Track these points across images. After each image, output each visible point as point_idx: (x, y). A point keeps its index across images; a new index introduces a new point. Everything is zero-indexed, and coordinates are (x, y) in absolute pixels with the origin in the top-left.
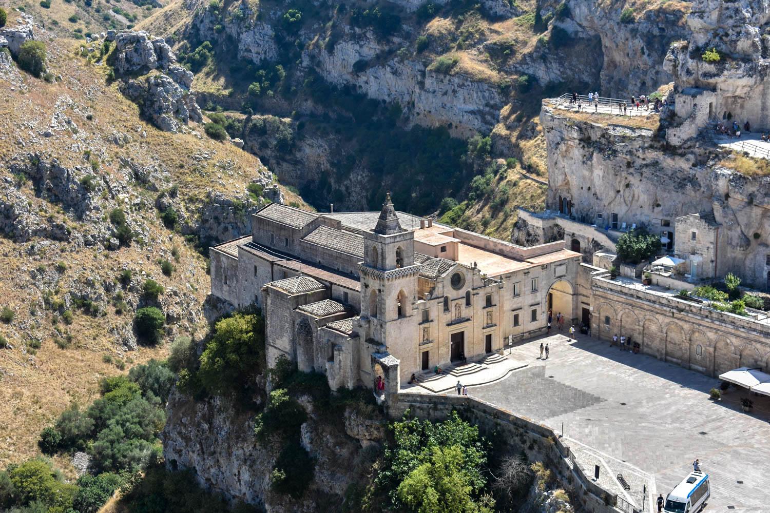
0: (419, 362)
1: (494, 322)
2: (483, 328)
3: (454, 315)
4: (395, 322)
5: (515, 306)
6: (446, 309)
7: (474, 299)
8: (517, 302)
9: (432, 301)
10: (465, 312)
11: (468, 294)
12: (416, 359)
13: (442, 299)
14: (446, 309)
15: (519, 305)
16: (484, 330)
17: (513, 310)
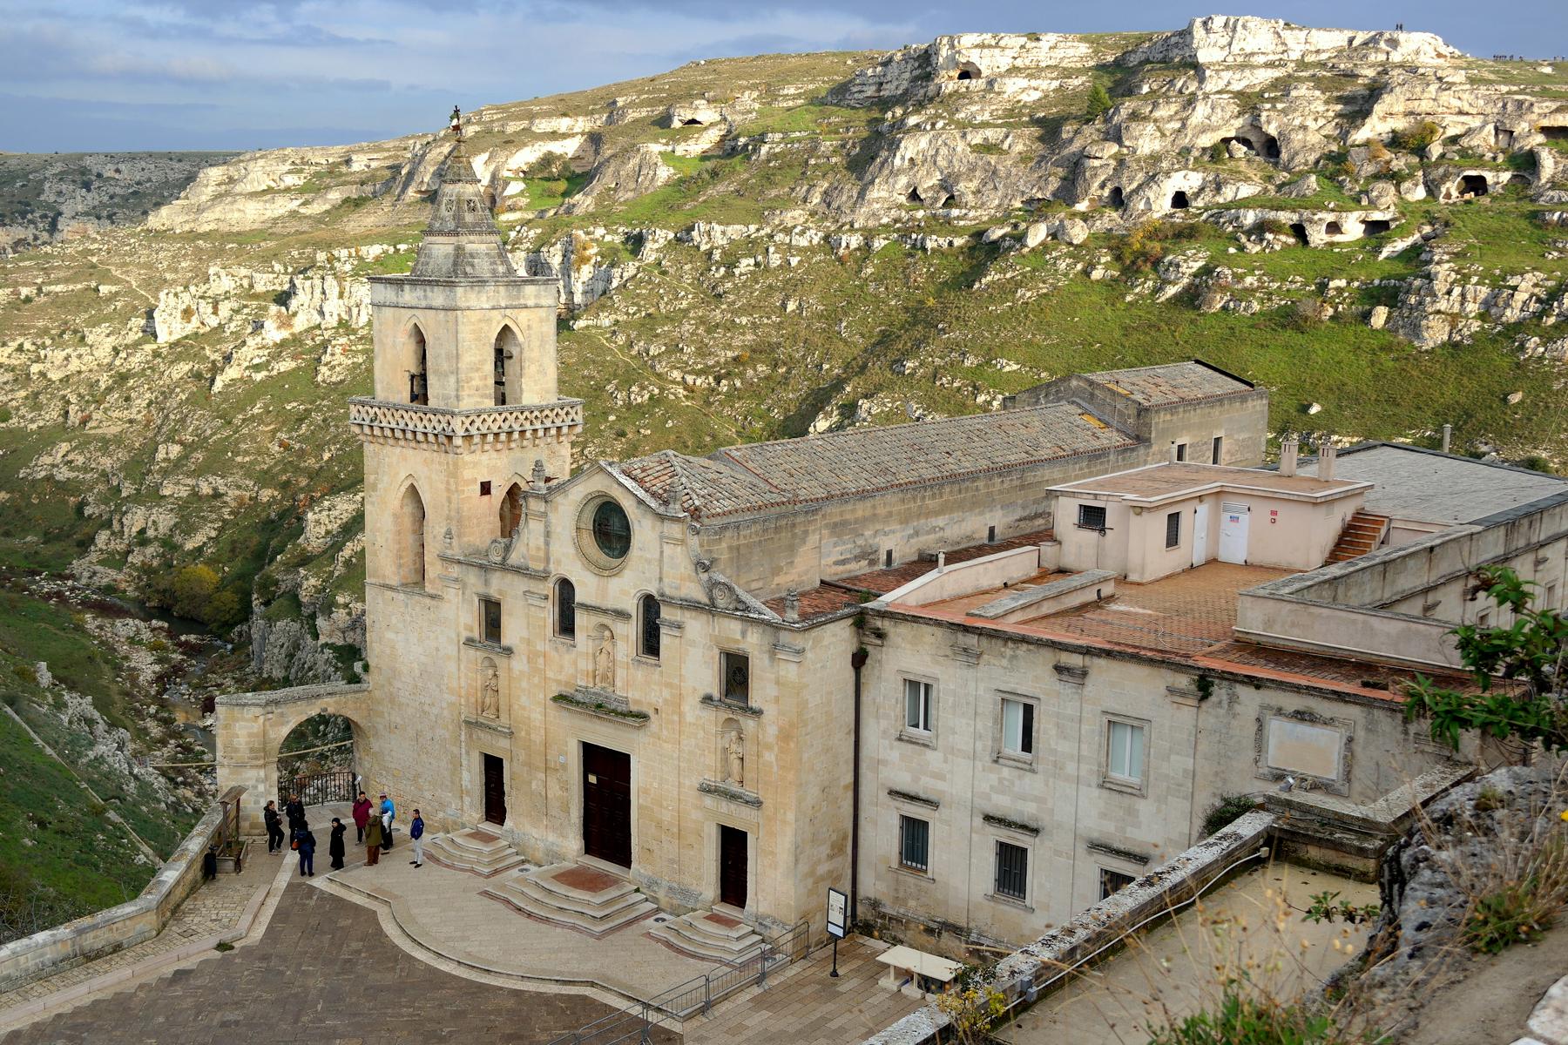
0: (473, 777)
1: (749, 792)
2: (706, 790)
3: (586, 665)
4: (389, 594)
5: (1002, 804)
6: (566, 626)
7: (666, 640)
8: (1019, 794)
9: (509, 577)
10: (635, 682)
11: (650, 606)
12: (456, 765)
13: (549, 588)
14: (566, 626)
15: (1025, 810)
16: (709, 801)
17: (988, 818)
